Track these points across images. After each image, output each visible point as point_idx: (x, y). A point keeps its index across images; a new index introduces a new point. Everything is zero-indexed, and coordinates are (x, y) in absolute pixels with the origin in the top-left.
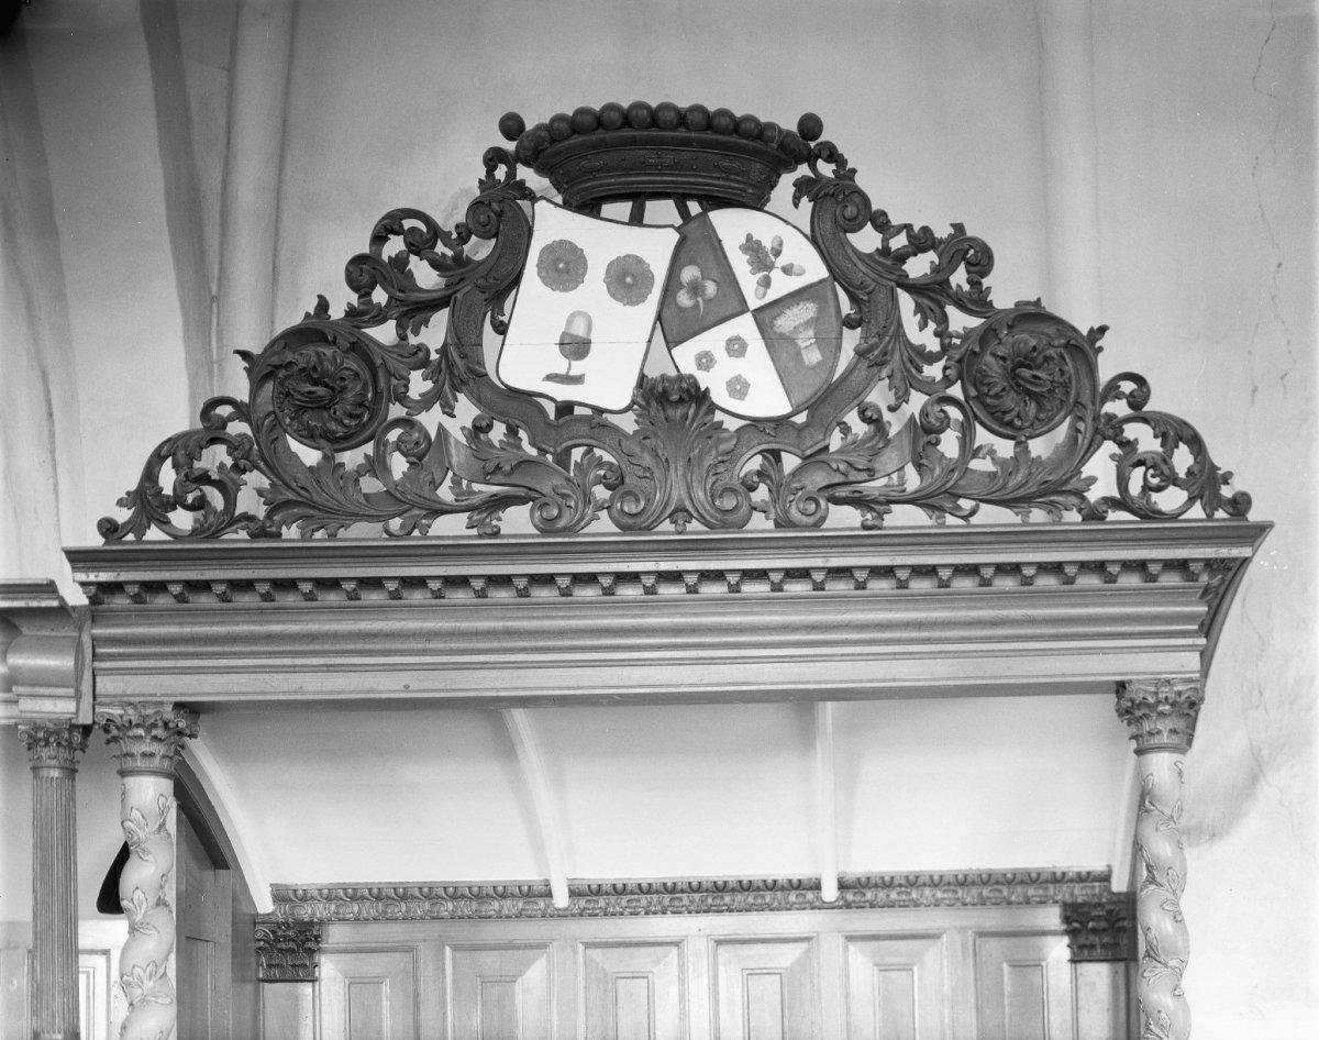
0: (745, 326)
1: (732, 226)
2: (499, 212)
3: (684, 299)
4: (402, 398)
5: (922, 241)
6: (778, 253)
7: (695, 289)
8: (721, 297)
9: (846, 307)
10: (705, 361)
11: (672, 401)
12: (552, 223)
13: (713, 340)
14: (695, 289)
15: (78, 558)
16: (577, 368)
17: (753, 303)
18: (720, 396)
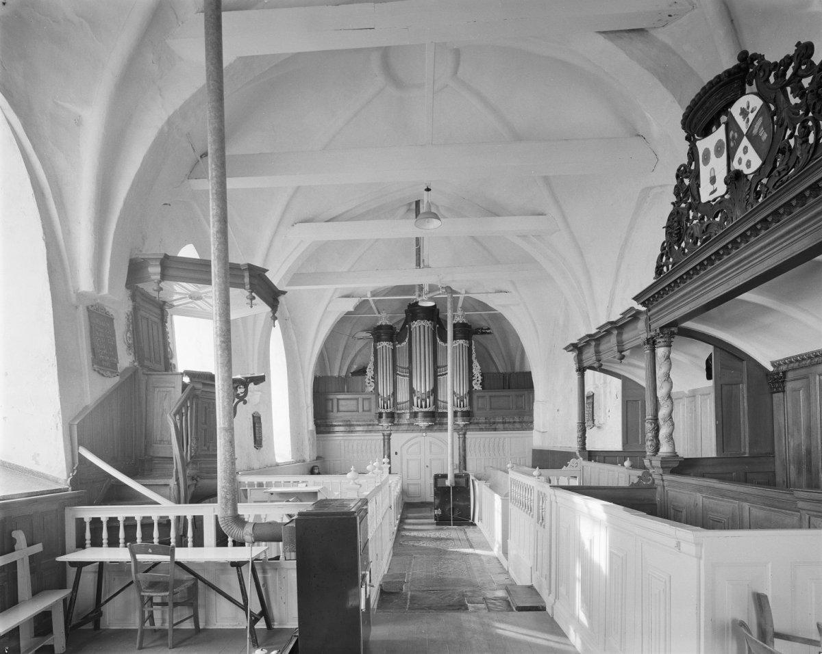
0: (745, 142)
1: (735, 110)
2: (693, 154)
3: (732, 144)
4: (688, 219)
5: (787, 61)
6: (748, 107)
7: (733, 137)
8: (739, 135)
9: (773, 108)
10: (740, 161)
11: (735, 178)
12: (703, 145)
13: (739, 153)
14: (733, 137)
15: (636, 298)
16: (715, 185)
17: (745, 131)
18: (746, 171)
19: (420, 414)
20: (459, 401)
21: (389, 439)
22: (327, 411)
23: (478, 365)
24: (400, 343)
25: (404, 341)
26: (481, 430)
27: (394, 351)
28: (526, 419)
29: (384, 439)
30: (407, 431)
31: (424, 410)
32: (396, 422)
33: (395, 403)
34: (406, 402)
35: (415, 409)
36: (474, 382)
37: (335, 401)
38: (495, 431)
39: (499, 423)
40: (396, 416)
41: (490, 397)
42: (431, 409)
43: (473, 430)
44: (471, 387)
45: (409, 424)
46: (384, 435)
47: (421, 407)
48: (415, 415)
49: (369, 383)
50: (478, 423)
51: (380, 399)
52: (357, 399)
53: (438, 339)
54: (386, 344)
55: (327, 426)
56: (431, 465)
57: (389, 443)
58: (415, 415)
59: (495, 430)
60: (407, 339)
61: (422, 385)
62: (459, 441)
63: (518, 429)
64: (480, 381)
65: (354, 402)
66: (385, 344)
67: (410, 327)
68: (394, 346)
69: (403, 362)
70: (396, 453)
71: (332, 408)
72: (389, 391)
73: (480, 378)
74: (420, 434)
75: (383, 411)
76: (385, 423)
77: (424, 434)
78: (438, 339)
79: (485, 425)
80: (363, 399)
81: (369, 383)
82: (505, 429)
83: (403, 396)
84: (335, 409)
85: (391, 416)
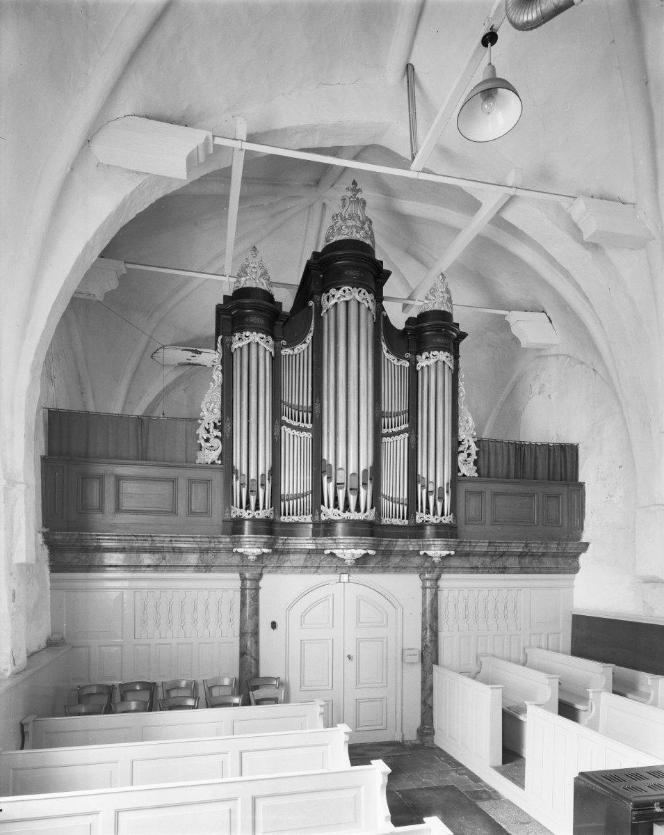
19: (340, 528)
20: (431, 498)
21: (257, 589)
22: (85, 509)
23: (471, 420)
24: (292, 343)
25: (300, 340)
26: (474, 570)
27: (276, 361)
28: (571, 547)
29: (243, 590)
30: (304, 568)
31: (353, 515)
32: (279, 546)
33: (276, 497)
34: (302, 496)
35: (329, 513)
36: (461, 457)
37: (110, 484)
38: (503, 573)
39: (512, 554)
40: (277, 528)
41: (496, 494)
42: (370, 515)
43: (456, 570)
44: (455, 468)
45: (309, 552)
46: (243, 579)
47: (347, 507)
48: (325, 529)
49: (207, 440)
50: (467, 555)
51: (236, 484)
52: (173, 481)
53: (384, 346)
54: (258, 339)
55: (85, 550)
56: (358, 652)
57: (256, 599)
58: (325, 529)
59: (503, 570)
60: (310, 337)
61: (349, 452)
62: (424, 595)
63: (549, 571)
64: (474, 457)
65: (165, 489)
66: (255, 337)
67: (319, 308)
68: (277, 349)
69: (298, 393)
70: (274, 625)
71: (102, 500)
72: (265, 465)
73: (474, 449)
74: (336, 577)
75: (245, 514)
76: (251, 547)
77: (345, 578)
78: (384, 346)
79: (482, 559)
80: (191, 481)
81: (207, 440)
82: (523, 570)
83: (295, 480)
84: (109, 504)
85: (270, 528)
